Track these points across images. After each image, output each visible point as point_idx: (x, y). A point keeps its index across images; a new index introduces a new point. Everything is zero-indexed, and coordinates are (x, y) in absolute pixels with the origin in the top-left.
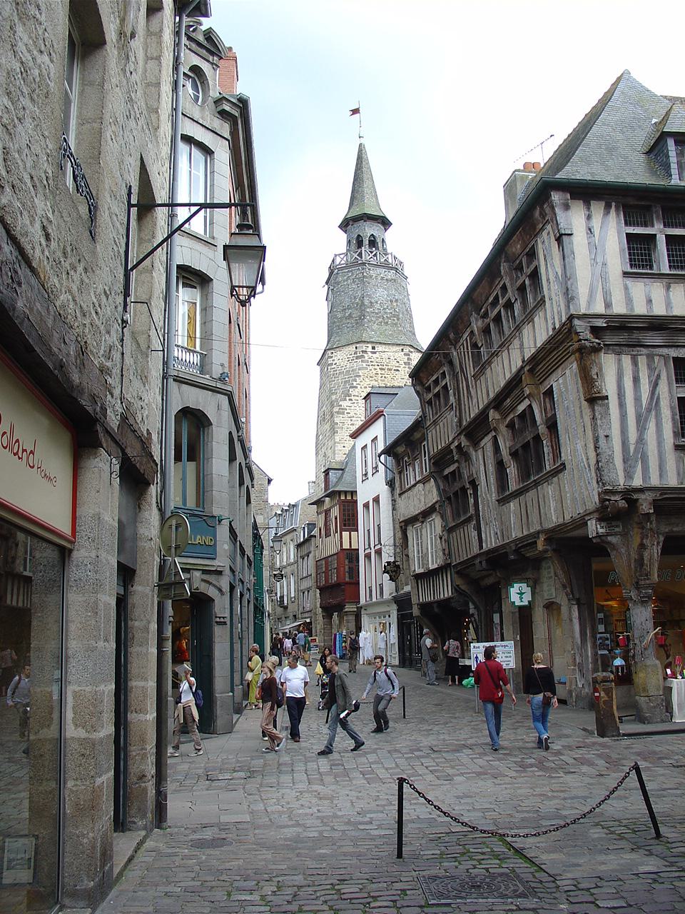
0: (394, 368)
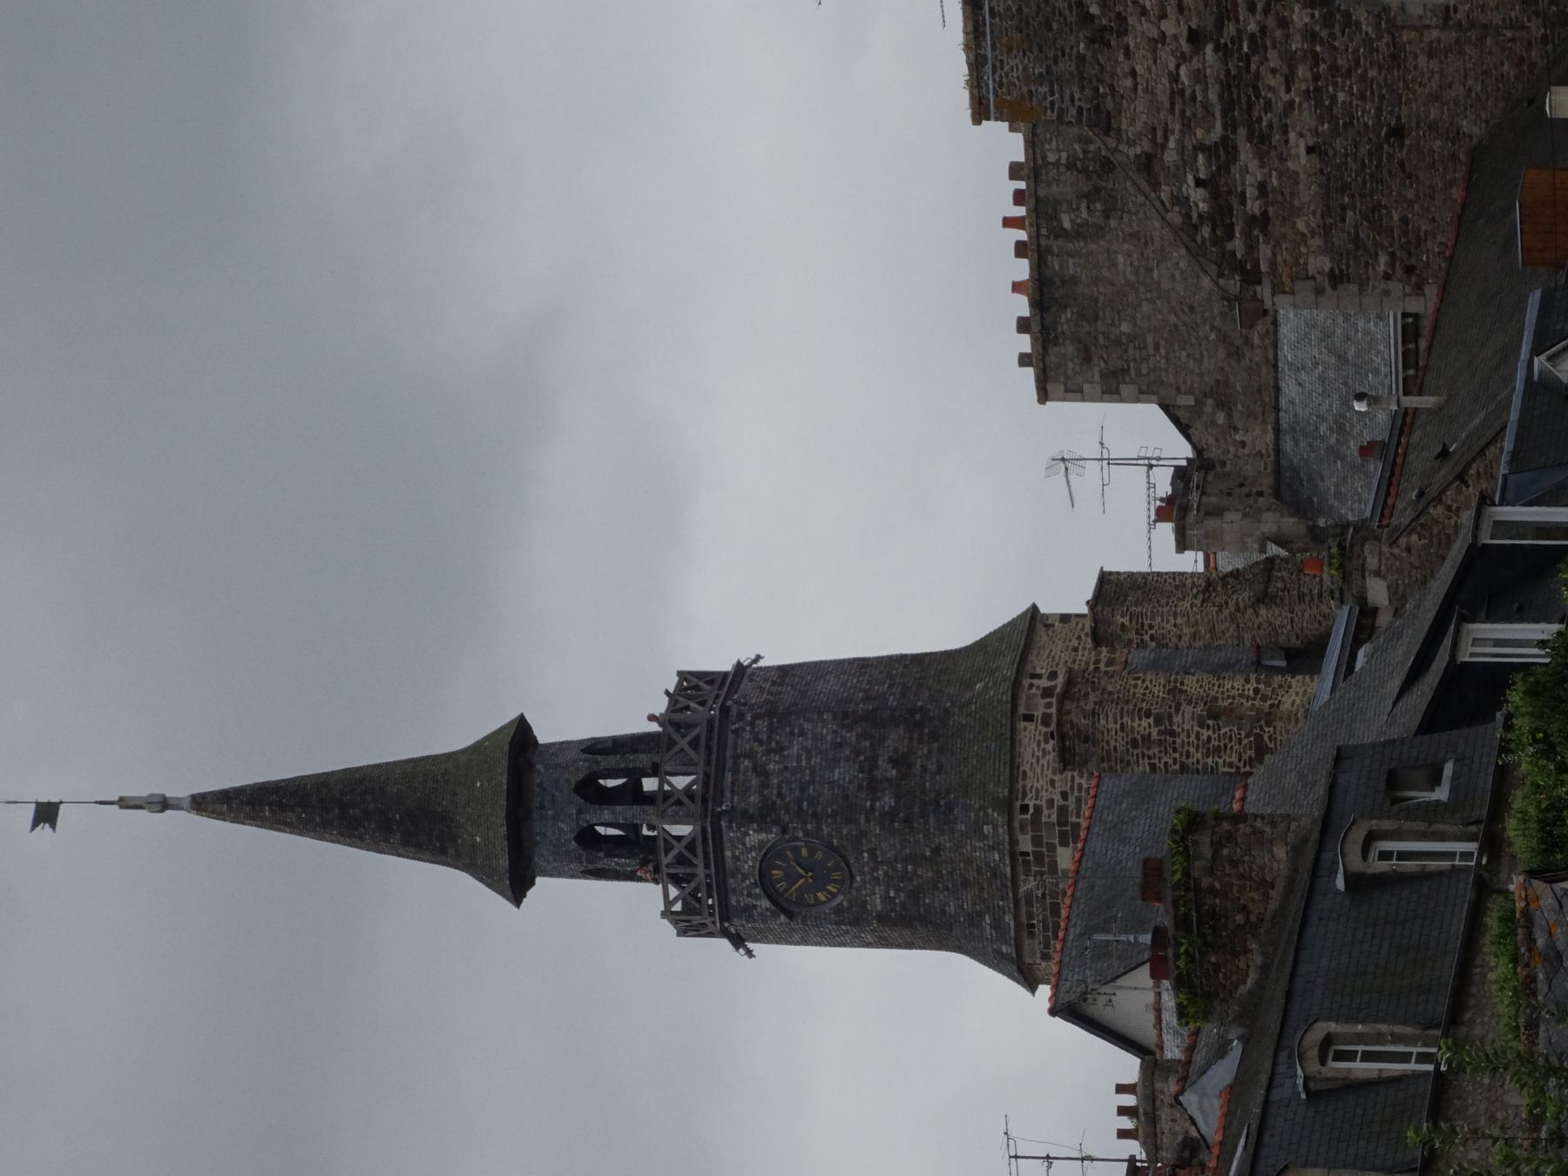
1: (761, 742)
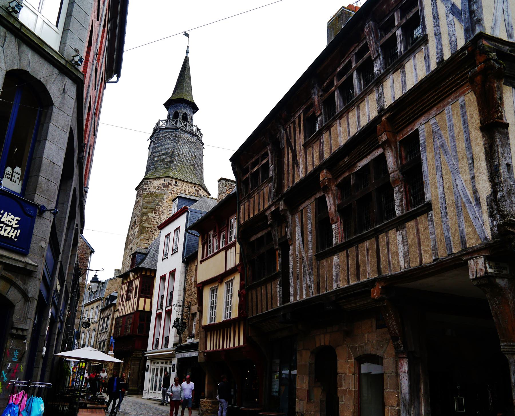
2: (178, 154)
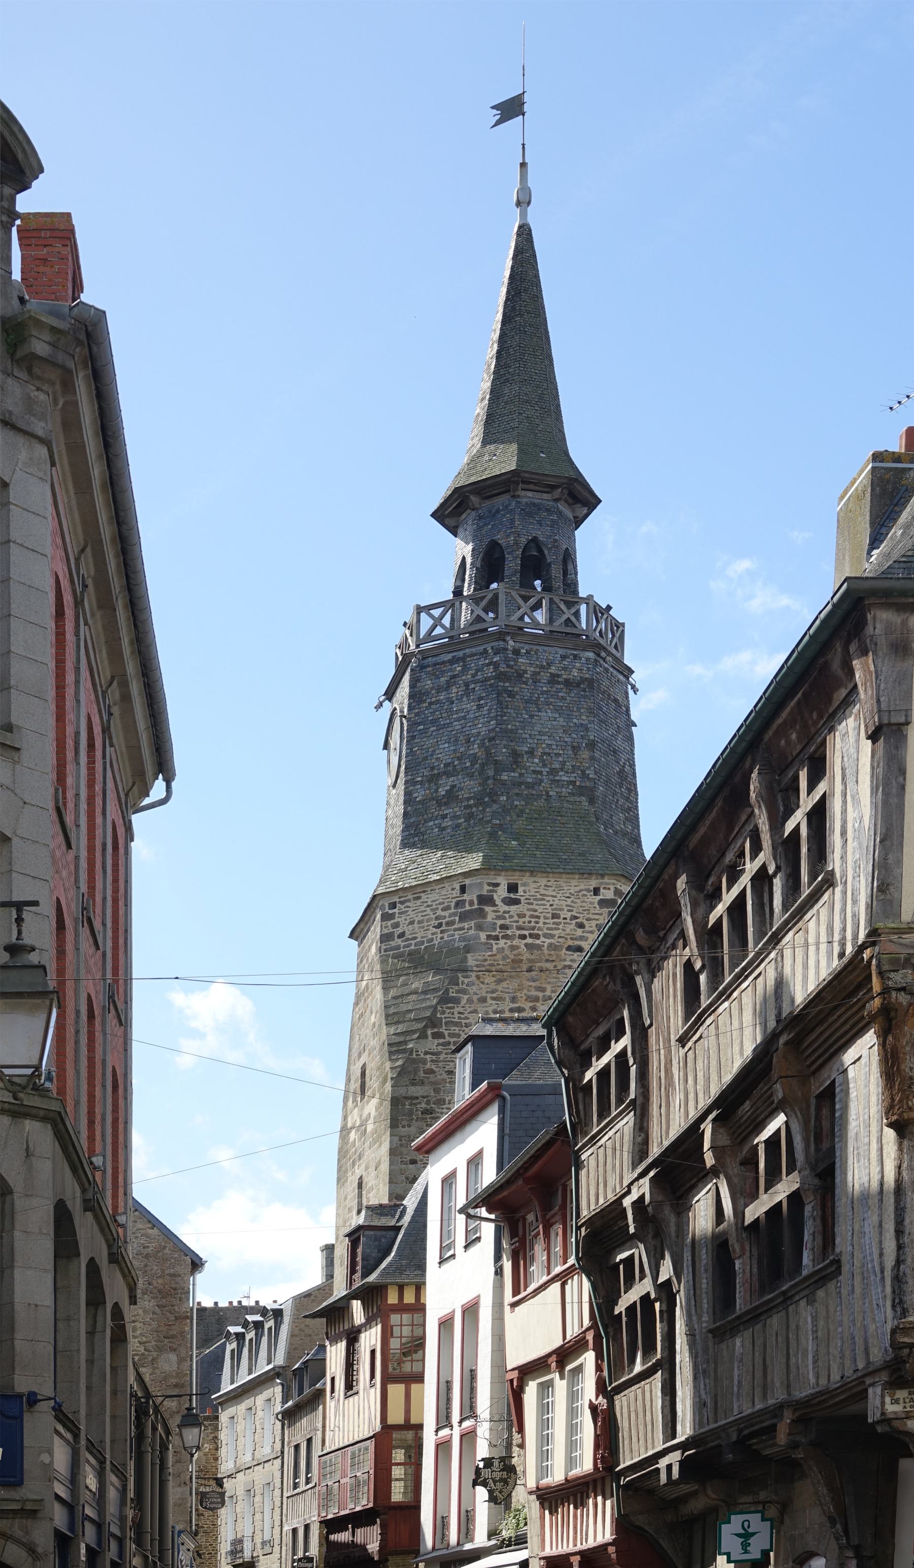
0: (570, 943)
1: (473, 676)
2: (515, 755)
